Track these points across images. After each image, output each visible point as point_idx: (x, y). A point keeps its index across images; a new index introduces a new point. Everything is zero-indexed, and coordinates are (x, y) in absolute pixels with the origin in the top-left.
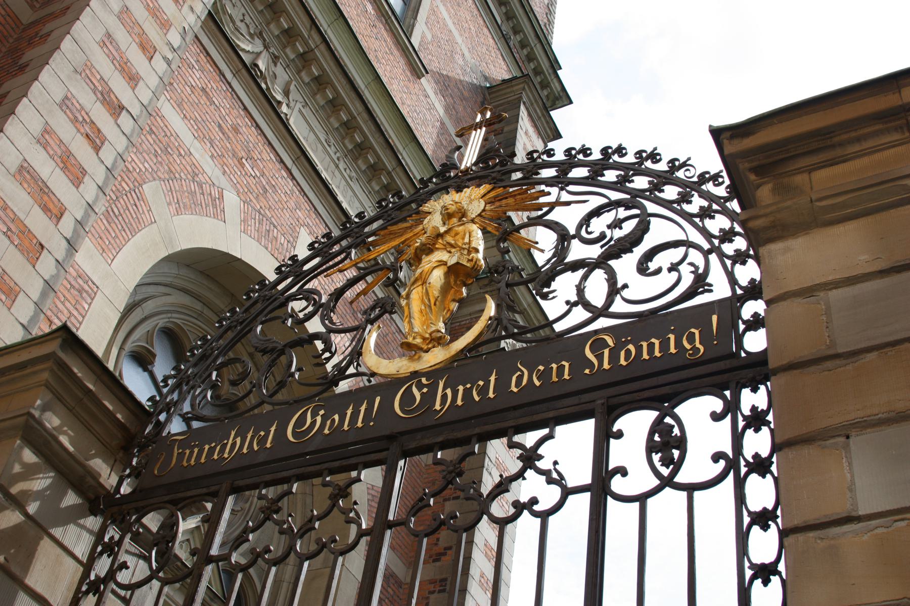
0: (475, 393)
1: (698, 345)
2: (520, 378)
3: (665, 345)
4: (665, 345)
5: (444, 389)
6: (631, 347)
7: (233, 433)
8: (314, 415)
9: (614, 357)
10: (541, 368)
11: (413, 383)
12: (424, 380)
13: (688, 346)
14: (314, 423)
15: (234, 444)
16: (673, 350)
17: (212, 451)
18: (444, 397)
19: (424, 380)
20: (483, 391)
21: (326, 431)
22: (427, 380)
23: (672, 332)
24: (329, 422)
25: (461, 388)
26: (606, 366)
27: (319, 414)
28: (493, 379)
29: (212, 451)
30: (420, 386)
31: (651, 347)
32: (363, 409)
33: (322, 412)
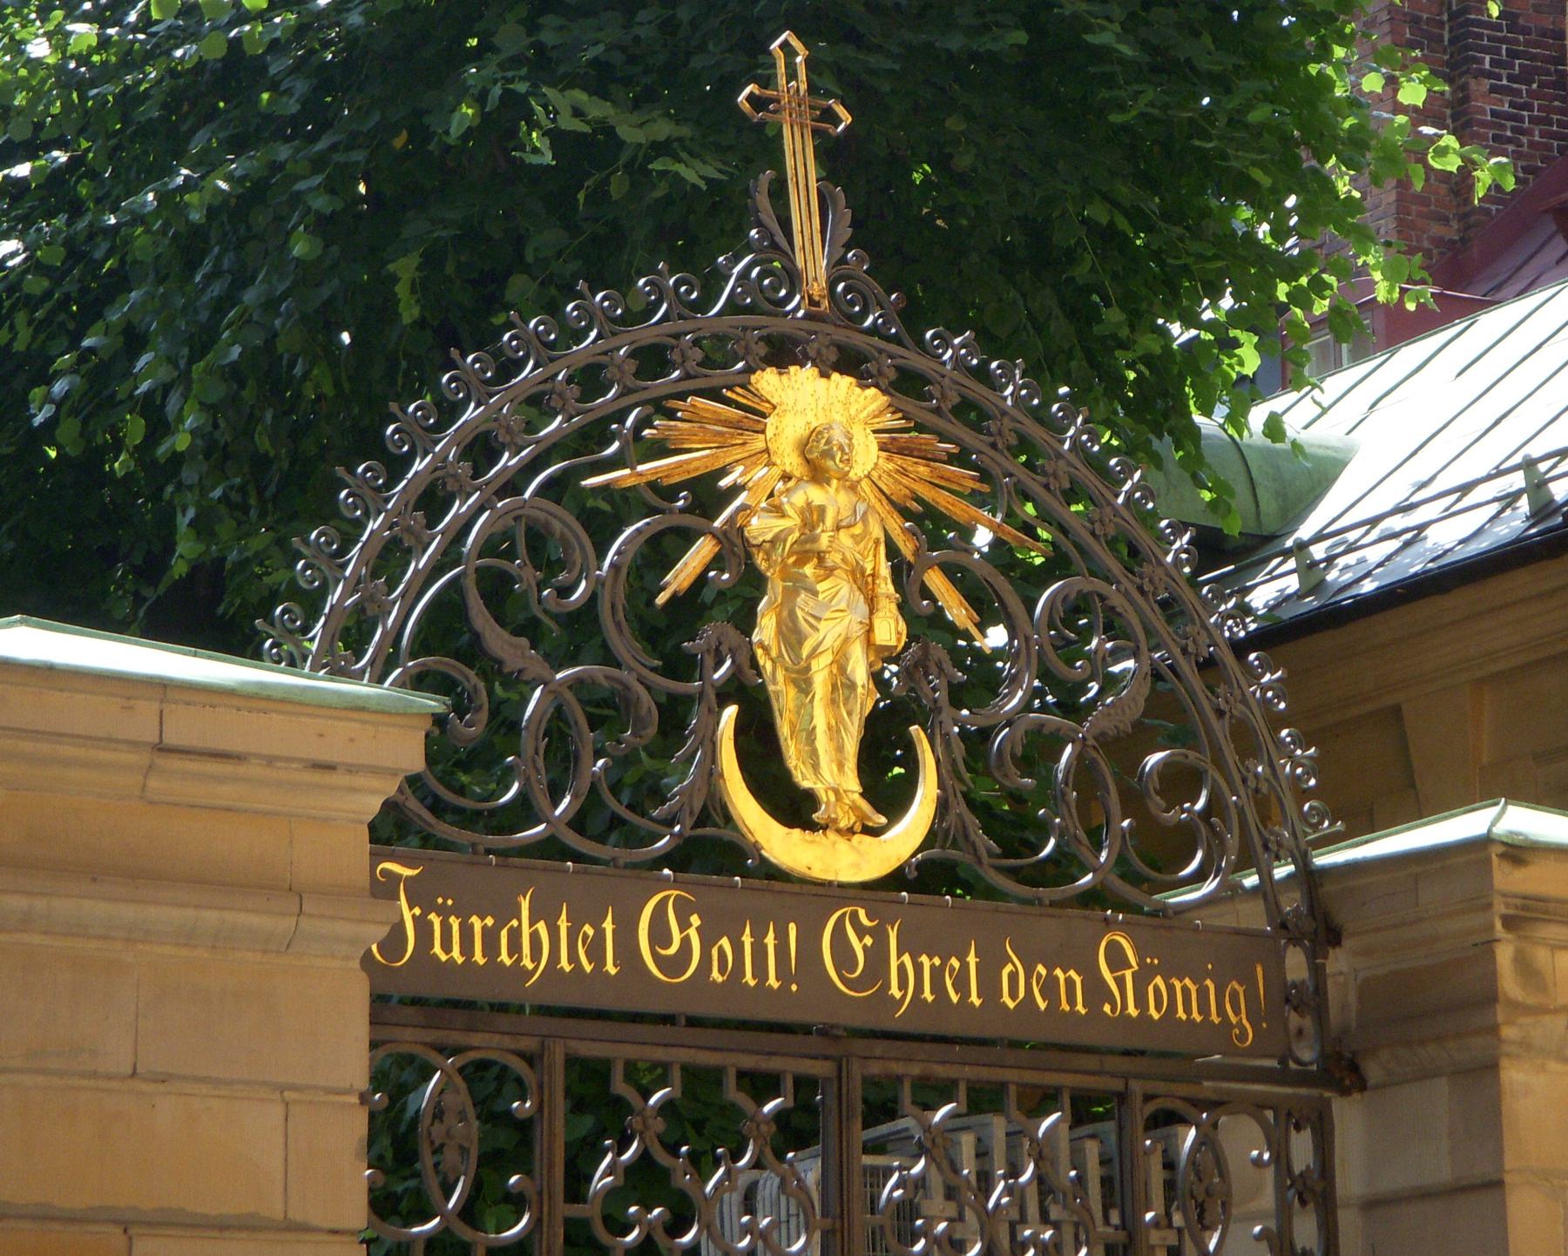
0: (949, 983)
1: (1245, 1021)
2: (1013, 977)
3: (1203, 994)
4: (1203, 994)
5: (899, 955)
6: (1159, 980)
7: (525, 905)
8: (684, 925)
9: (1141, 1001)
10: (1041, 969)
11: (844, 914)
12: (862, 913)
13: (1234, 1020)
14: (686, 942)
15: (535, 939)
16: (1215, 1019)
17: (490, 938)
18: (902, 969)
19: (862, 913)
20: (961, 984)
21: (716, 975)
22: (870, 917)
23: (1208, 975)
24: (715, 952)
25: (924, 959)
26: (1132, 1011)
27: (691, 925)
28: (972, 959)
29: (490, 938)
30: (861, 931)
31: (1185, 991)
32: (770, 940)
33: (695, 920)
